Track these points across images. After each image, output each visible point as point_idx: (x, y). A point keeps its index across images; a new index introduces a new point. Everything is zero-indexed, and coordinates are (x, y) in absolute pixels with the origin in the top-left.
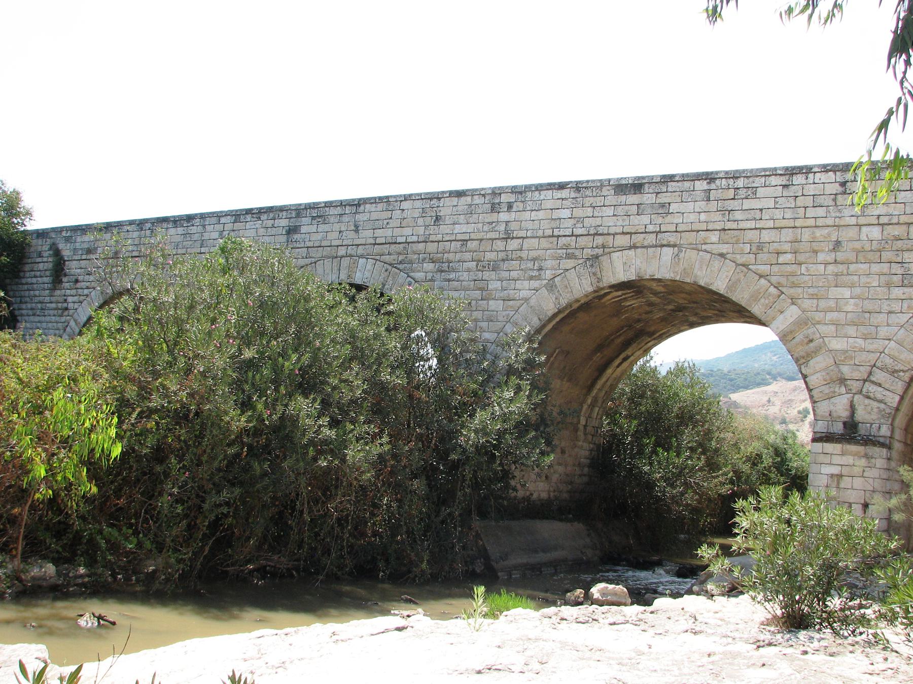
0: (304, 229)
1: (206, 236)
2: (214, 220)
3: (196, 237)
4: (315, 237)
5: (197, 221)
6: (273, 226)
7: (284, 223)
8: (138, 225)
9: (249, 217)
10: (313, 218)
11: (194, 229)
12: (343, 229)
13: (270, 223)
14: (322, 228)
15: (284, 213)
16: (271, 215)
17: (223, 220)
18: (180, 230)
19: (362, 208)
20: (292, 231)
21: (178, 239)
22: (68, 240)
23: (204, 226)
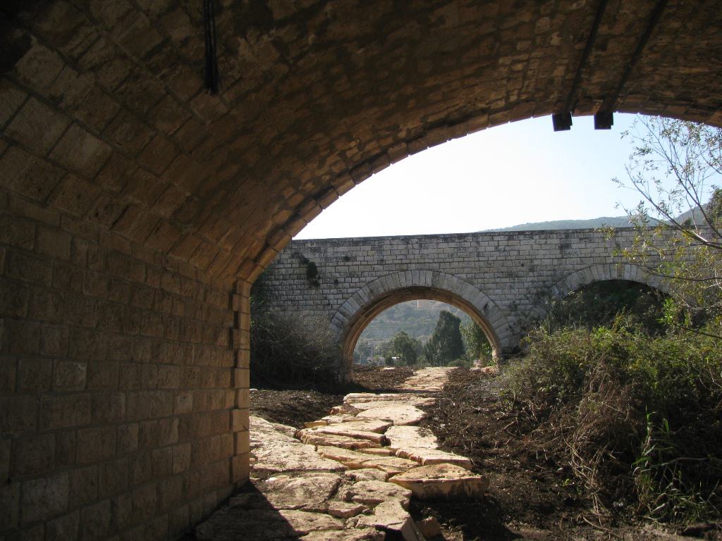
0: (574, 246)
1: (481, 249)
2: (486, 238)
3: (471, 249)
4: (584, 251)
5: (470, 238)
6: (546, 243)
7: (556, 241)
8: (403, 240)
9: (522, 237)
10: (581, 239)
11: (467, 244)
12: (607, 246)
13: (543, 241)
14: (589, 245)
15: (555, 235)
16: (543, 236)
17: (495, 238)
18: (453, 245)
19: (619, 234)
20: (563, 247)
21: (451, 251)
22: (314, 251)
23: (478, 242)
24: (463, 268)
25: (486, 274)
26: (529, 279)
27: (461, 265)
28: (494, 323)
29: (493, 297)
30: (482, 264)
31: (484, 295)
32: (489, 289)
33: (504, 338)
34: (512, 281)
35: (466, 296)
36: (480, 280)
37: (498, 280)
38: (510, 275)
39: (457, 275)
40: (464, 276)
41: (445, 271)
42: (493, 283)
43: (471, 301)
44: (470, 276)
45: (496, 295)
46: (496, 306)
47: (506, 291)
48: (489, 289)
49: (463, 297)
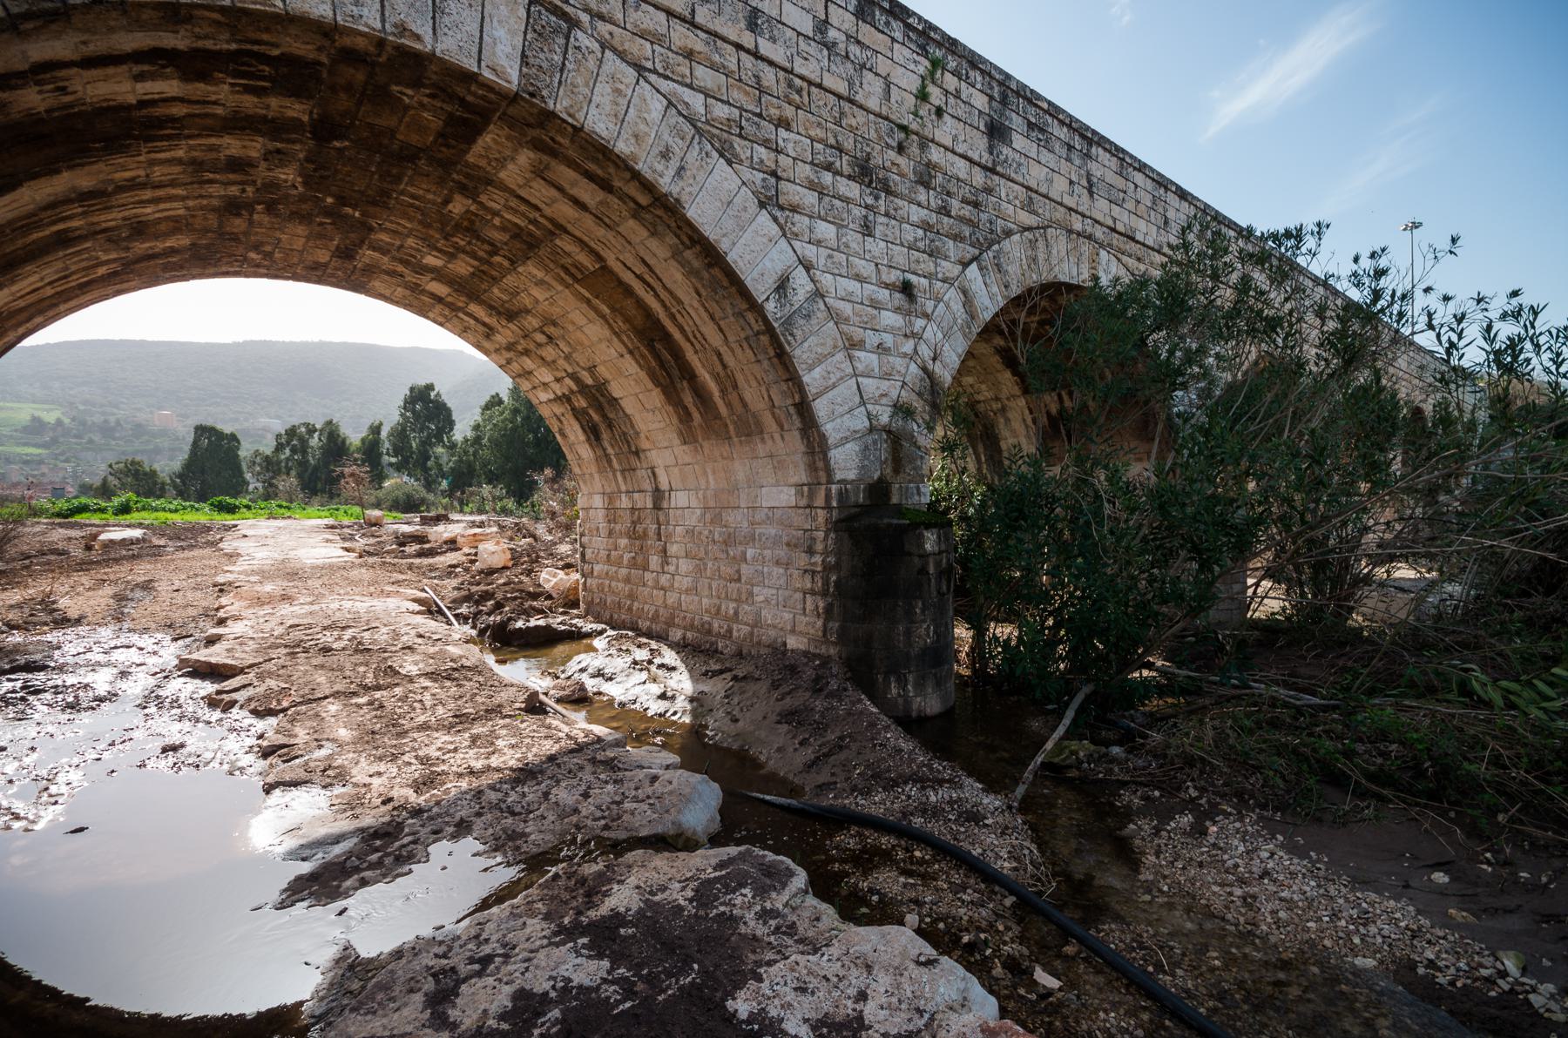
24: (689, 55)
25: (783, 133)
26: (917, 214)
27: (680, 35)
28: (811, 369)
29: (810, 252)
30: (769, 76)
31: (774, 230)
32: (794, 209)
33: (844, 441)
34: (870, 201)
35: (702, 212)
36: (761, 152)
37: (827, 178)
38: (864, 172)
39: (665, 86)
40: (697, 102)
41: (604, 28)
42: (811, 186)
43: (724, 246)
44: (721, 111)
45: (818, 243)
46: (818, 294)
47: (853, 238)
48: (794, 209)
49: (692, 213)
